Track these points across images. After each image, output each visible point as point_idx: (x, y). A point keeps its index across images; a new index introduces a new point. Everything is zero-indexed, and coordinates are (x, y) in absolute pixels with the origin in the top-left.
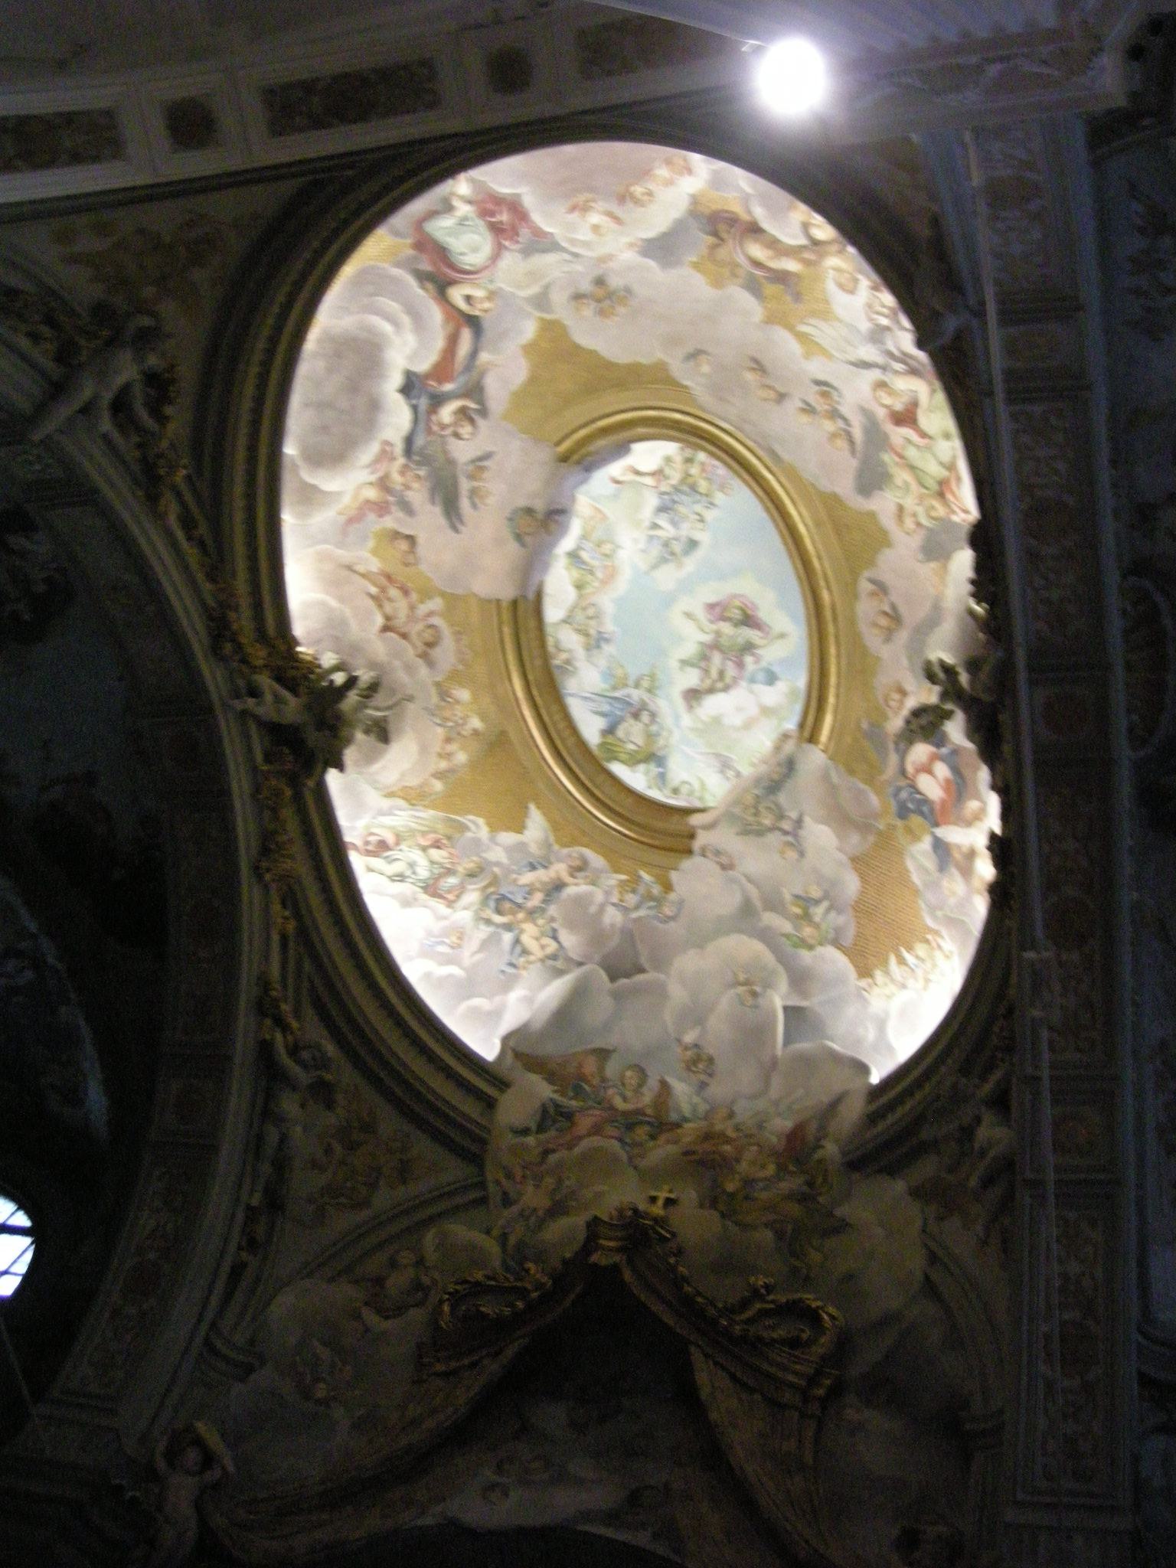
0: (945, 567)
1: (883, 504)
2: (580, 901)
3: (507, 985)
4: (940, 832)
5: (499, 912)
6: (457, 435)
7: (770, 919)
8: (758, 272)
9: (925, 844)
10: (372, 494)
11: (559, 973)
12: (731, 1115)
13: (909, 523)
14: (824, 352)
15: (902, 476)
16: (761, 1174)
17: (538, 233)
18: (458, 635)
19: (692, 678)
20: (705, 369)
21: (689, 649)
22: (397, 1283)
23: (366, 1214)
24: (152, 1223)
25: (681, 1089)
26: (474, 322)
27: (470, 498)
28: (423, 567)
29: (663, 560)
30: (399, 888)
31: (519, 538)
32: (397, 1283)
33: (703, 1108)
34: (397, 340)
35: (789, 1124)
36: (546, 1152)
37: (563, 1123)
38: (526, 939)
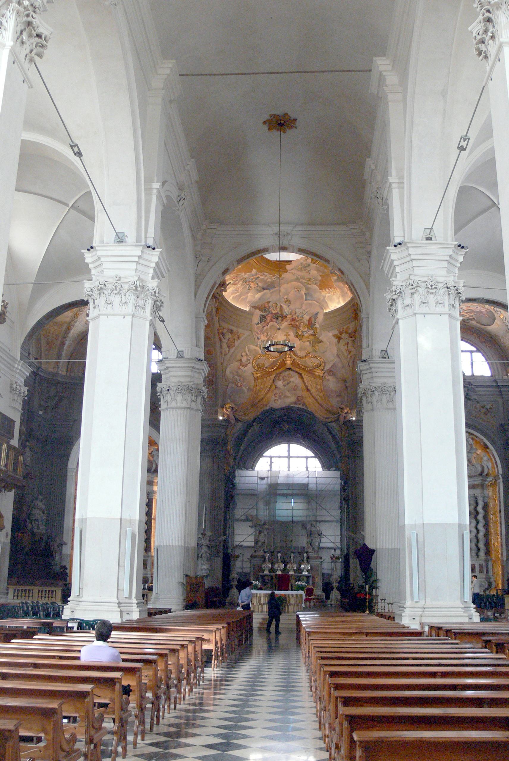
3: (248, 293)
11: (260, 291)
12: (296, 313)
16: (305, 330)
22: (244, 359)
23: (234, 348)
25: (285, 307)
35: (308, 318)
36: (263, 327)
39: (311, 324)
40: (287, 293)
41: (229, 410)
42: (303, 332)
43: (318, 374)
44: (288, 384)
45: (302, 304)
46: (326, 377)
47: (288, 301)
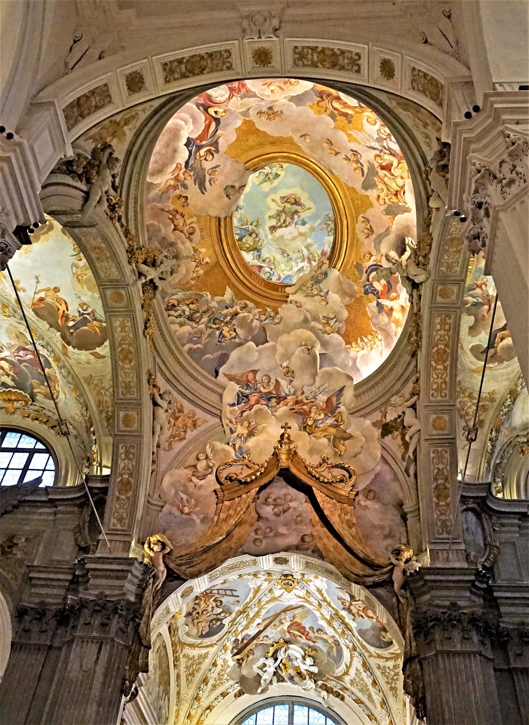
0: (394, 218)
1: (372, 194)
2: (244, 318)
4: (380, 300)
5: (214, 324)
6: (205, 159)
7: (313, 324)
8: (336, 112)
9: (375, 303)
10: (172, 182)
12: (303, 393)
13: (381, 201)
14: (356, 140)
15: (381, 186)
16: (319, 418)
17: (248, 91)
18: (202, 230)
19: (273, 222)
20: (308, 140)
21: (273, 212)
22: (201, 465)
23: (184, 442)
24: (122, 465)
25: (283, 383)
26: (218, 121)
27: (210, 181)
28: (190, 206)
29: (265, 181)
30: (178, 320)
31: (227, 196)
32: (201, 465)
33: (292, 390)
34: (186, 127)
35: (325, 398)
36: (242, 412)
37: (245, 400)
38: (224, 332)
39: (330, 408)
40: (287, 356)
41: (156, 548)
42: (315, 421)
43: (343, 493)
44: (285, 511)
45: (314, 375)
46: (362, 503)
47: (289, 373)
